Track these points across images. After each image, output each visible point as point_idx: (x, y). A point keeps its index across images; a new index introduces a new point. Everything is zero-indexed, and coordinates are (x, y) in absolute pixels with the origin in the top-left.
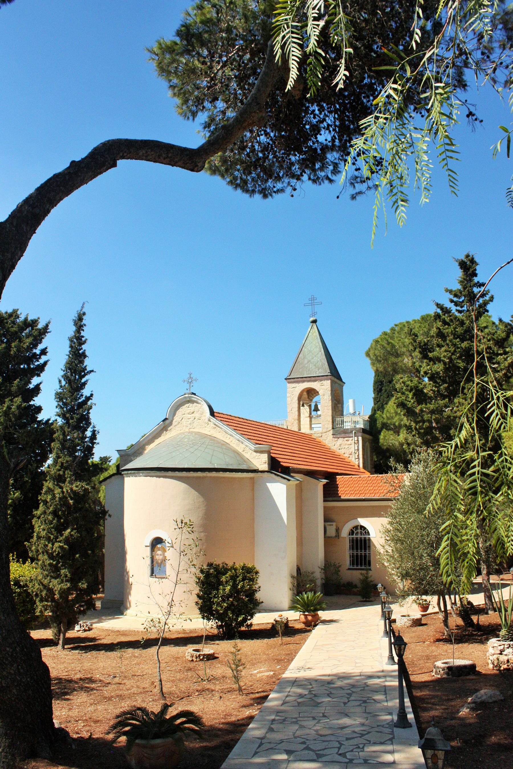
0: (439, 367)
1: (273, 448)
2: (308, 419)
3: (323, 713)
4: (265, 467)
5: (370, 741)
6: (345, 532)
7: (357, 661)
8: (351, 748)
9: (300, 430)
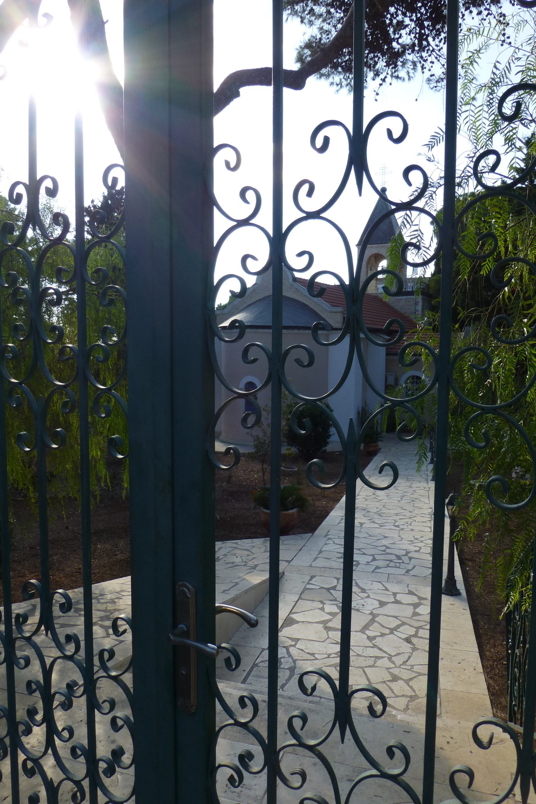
3: (383, 506)
5: (415, 521)
8: (403, 523)
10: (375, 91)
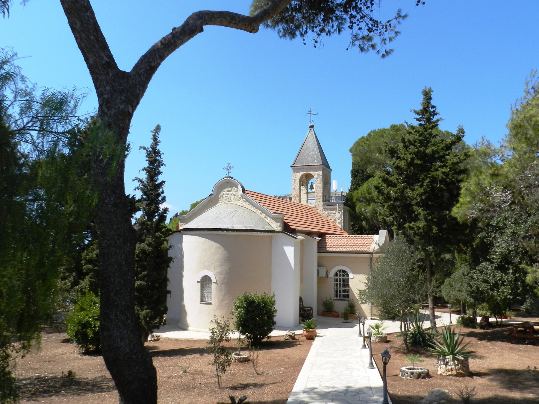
0: (402, 164)
1: (285, 216)
2: (306, 195)
4: (280, 229)
6: (332, 274)
7: (348, 365)
9: (300, 202)
10: (314, 40)
